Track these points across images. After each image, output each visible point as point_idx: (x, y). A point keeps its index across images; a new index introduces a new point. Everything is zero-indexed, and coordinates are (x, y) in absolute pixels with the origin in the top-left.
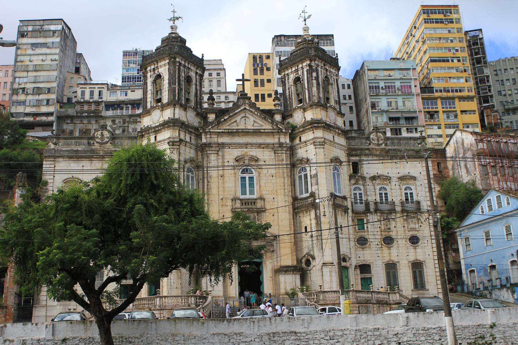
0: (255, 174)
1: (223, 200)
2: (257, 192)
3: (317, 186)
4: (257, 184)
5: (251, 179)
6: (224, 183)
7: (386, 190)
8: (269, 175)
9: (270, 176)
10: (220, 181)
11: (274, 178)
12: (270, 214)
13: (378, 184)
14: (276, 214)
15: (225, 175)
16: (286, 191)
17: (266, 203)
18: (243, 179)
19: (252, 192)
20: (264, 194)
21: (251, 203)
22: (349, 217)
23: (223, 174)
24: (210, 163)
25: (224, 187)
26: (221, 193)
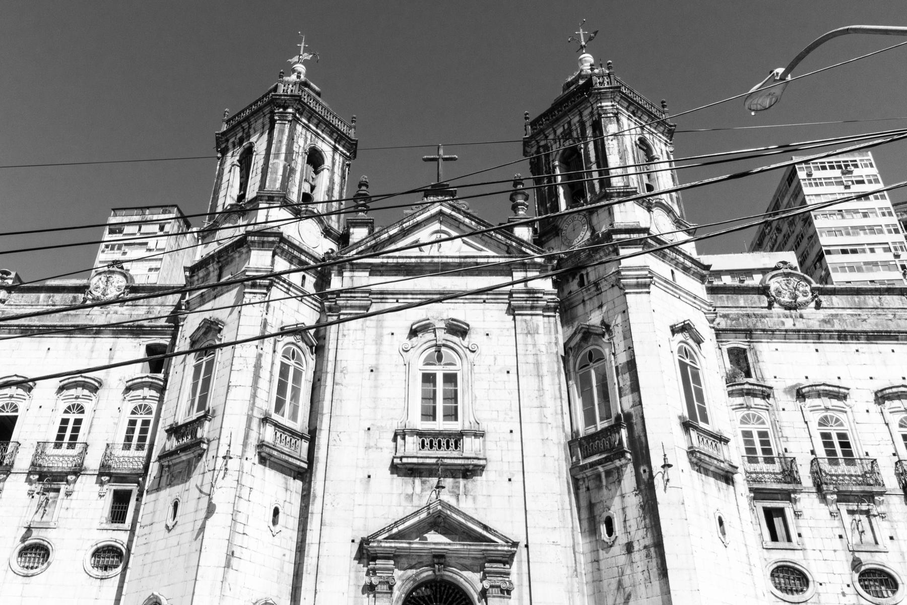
0: (460, 368)
3: (636, 394)
5: (451, 379)
6: (376, 387)
7: (842, 425)
9: (500, 371)
13: (814, 409)
15: (381, 367)
16: (548, 412)
17: (489, 445)
18: (428, 378)
19: (452, 414)
21: (448, 442)
22: (739, 496)
23: (377, 365)
24: (344, 335)
25: (375, 399)
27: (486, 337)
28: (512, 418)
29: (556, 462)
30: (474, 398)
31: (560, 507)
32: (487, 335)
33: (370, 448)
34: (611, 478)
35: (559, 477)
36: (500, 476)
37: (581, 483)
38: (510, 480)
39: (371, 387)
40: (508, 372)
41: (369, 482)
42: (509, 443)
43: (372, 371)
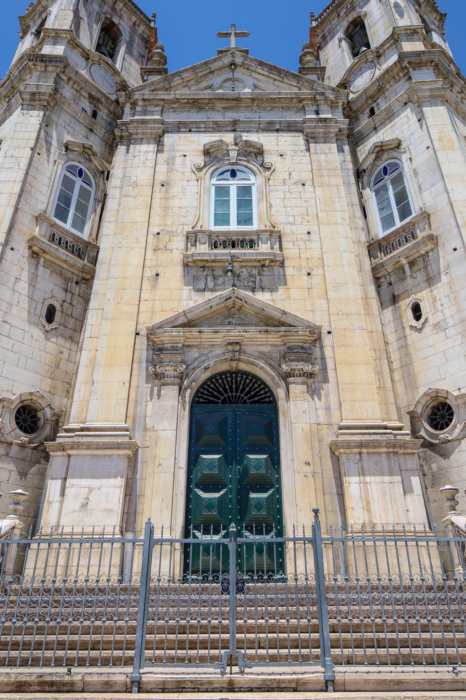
1: (160, 236)
2: (260, 218)
4: (259, 201)
6: (167, 199)
8: (293, 181)
9: (296, 183)
10: (157, 195)
11: (308, 187)
12: (299, 269)
14: (317, 272)
15: (172, 182)
20: (281, 224)
26: (155, 220)
27: (280, 157)
28: (309, 222)
29: (357, 258)
30: (268, 206)
31: (364, 297)
32: (281, 155)
33: (159, 249)
34: (416, 266)
35: (361, 271)
36: (298, 271)
37: (383, 280)
38: (309, 274)
39: (161, 199)
40: (303, 185)
41: (157, 279)
42: (307, 243)
43: (163, 185)
